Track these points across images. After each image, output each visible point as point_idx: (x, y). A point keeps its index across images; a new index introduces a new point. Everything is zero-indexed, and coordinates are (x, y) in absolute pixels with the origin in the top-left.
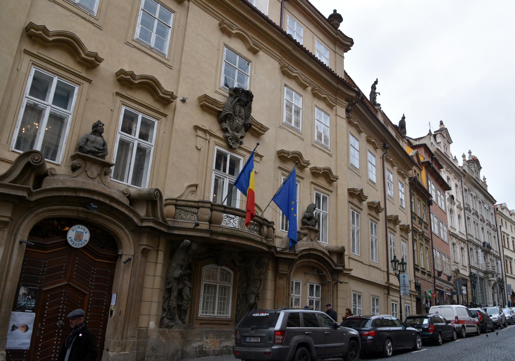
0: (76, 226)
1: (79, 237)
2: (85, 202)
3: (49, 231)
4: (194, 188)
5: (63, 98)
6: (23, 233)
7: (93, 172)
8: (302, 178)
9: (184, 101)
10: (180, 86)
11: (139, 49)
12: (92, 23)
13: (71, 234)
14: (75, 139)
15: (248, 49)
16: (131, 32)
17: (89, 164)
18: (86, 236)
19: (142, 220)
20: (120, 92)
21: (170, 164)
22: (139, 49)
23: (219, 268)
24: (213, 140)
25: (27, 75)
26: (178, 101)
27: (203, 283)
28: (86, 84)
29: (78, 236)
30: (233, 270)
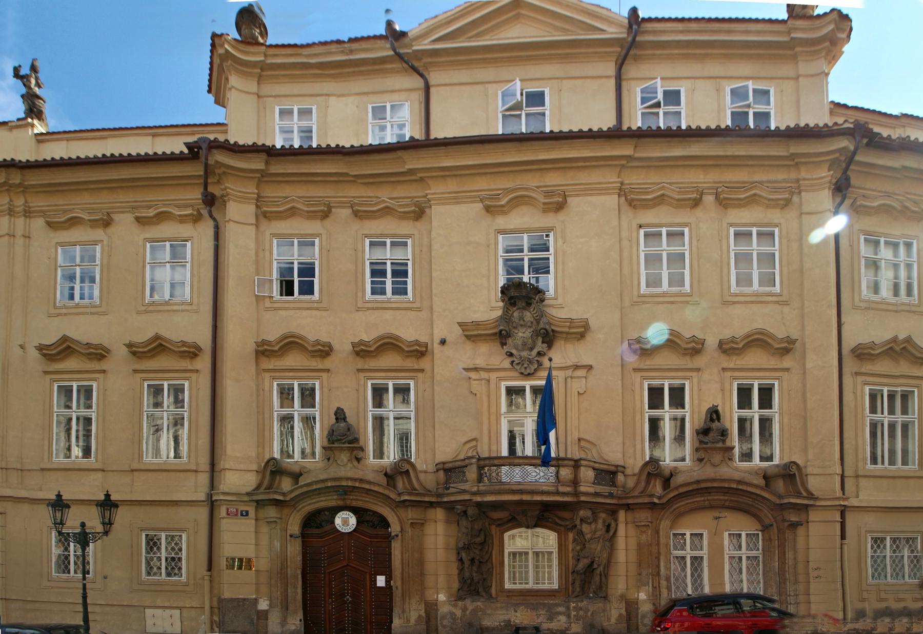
0: (341, 513)
1: (345, 522)
2: (346, 491)
3: (316, 523)
4: (474, 443)
5: (308, 396)
6: (295, 527)
7: (342, 461)
8: (698, 370)
9: (443, 342)
10: (435, 326)
11: (373, 309)
12: (317, 309)
13: (338, 521)
14: (326, 433)
15: (545, 211)
16: (360, 294)
17: (337, 453)
18: (353, 521)
19: (400, 494)
20: (359, 367)
21: (437, 426)
22: (373, 309)
23: (530, 530)
24: (493, 376)
25: (271, 391)
26: (436, 345)
27: (506, 552)
28: (325, 375)
29: (346, 522)
30: (555, 531)
